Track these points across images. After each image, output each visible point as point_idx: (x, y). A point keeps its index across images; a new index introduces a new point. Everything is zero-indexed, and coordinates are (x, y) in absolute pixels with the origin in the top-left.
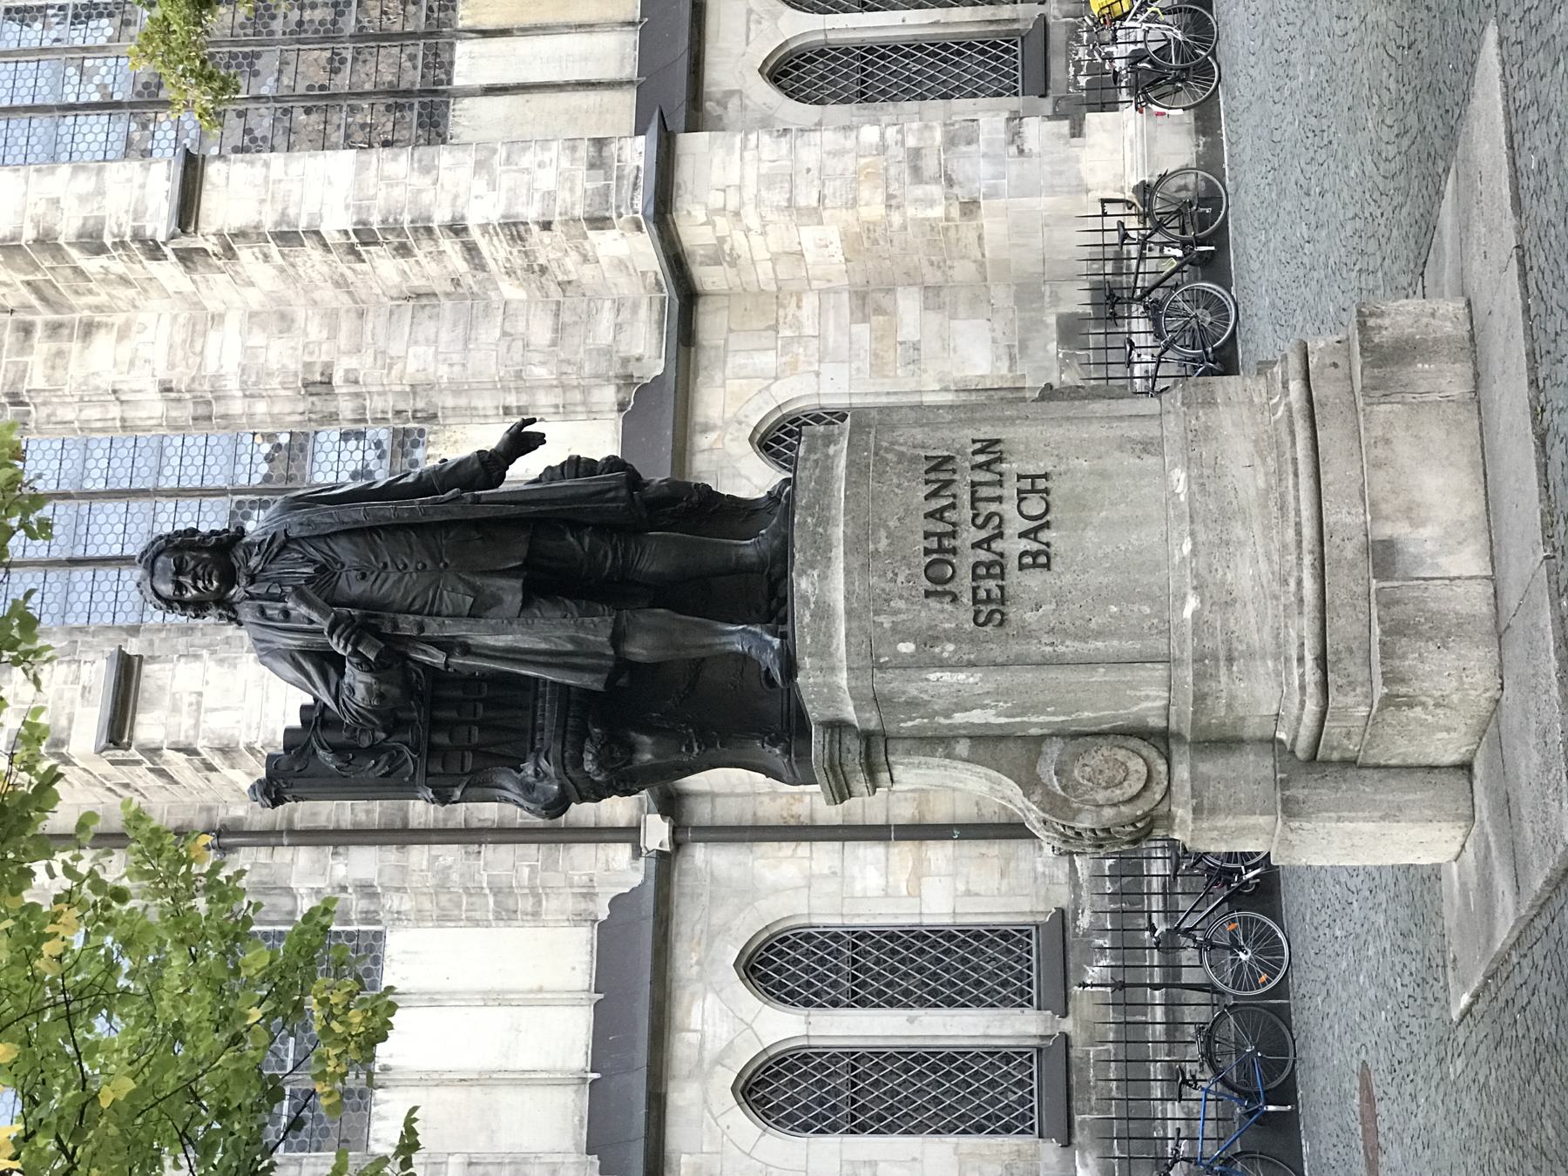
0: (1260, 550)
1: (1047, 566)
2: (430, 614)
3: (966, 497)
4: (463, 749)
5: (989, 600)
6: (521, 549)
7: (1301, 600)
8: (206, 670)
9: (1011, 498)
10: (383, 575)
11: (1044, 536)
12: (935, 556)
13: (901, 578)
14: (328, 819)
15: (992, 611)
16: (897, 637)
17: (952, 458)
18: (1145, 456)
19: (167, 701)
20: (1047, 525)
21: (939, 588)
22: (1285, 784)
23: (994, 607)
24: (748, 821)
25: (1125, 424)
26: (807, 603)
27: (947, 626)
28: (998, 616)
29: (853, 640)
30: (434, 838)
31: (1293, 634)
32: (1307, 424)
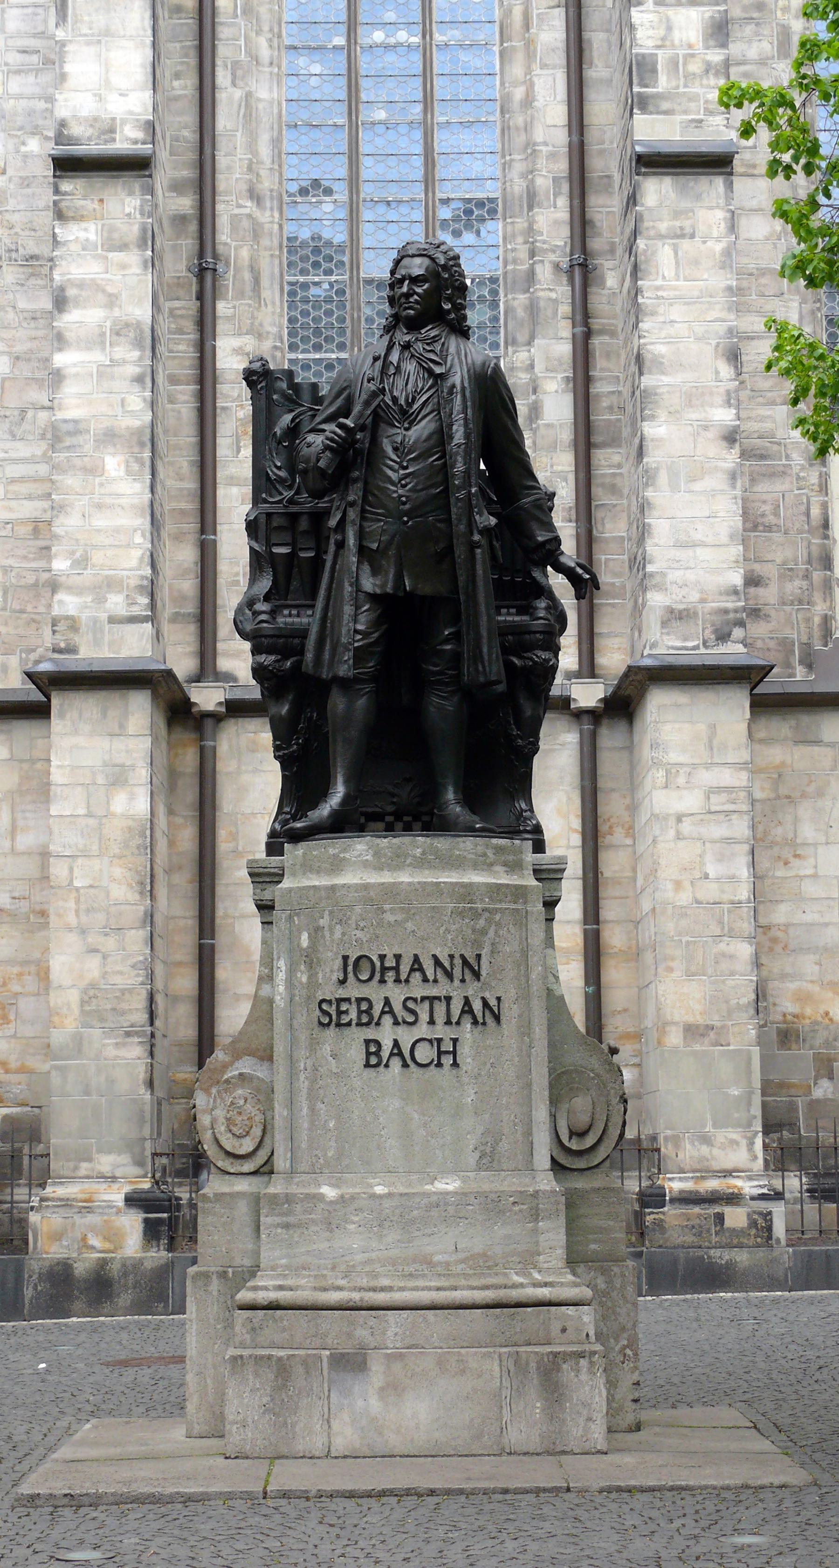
0: (374, 1255)
1: (367, 1065)
2: (363, 511)
3: (434, 992)
4: (293, 544)
5: (340, 1013)
6: (426, 589)
7: (325, 1290)
8: (718, 240)
9: (433, 1032)
10: (396, 466)
11: (396, 1063)
12: (378, 964)
13: (359, 934)
14: (603, 370)
15: (331, 1016)
16: (312, 931)
17: (479, 980)
18: (477, 1155)
19: (685, 204)
20: (405, 1065)
21: (350, 968)
22: (223, 1275)
23: (334, 1017)
24: (602, 783)
25: (519, 1136)
26: (345, 850)
27: (320, 975)
28: (326, 1020)
29: (312, 892)
30: (582, 475)
31: (303, 1282)
32: (489, 1301)
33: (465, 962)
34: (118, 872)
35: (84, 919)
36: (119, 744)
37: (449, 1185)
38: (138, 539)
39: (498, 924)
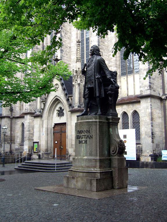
6: (91, 86)
33: (88, 131)
34: (148, 118)
35: (145, 124)
36: (147, 104)
37: (85, 158)
38: (148, 80)
39: (92, 126)
